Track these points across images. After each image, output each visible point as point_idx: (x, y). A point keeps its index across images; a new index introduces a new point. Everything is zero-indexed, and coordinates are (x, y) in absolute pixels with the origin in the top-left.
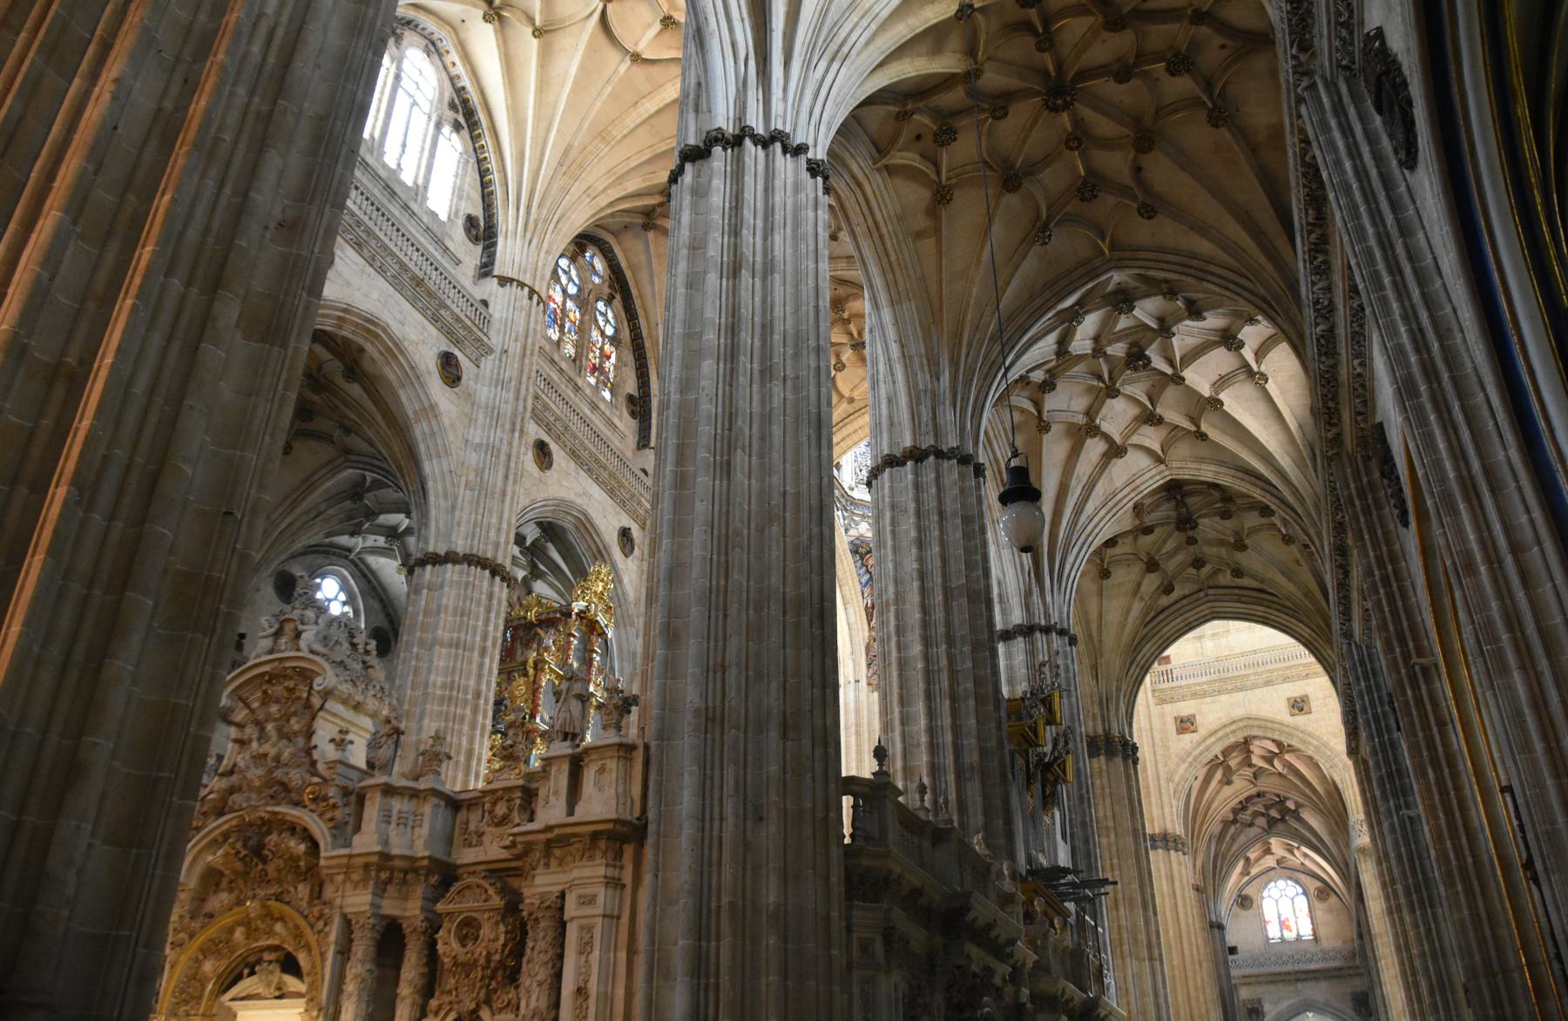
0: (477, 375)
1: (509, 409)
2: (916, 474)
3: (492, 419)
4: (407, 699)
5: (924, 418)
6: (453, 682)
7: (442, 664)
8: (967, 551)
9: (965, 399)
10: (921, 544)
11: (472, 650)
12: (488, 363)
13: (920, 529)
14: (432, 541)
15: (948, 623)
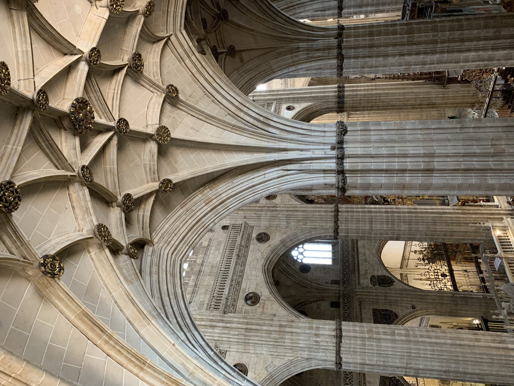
0: (257, 226)
1: (268, 213)
2: (350, 58)
3: (276, 219)
4: (391, 236)
5: (321, 54)
6: (386, 222)
7: (385, 226)
8: (387, 34)
9: (309, 35)
10: (386, 56)
11: (372, 216)
12: (251, 223)
13: (378, 56)
14: (329, 234)
15: (425, 43)
